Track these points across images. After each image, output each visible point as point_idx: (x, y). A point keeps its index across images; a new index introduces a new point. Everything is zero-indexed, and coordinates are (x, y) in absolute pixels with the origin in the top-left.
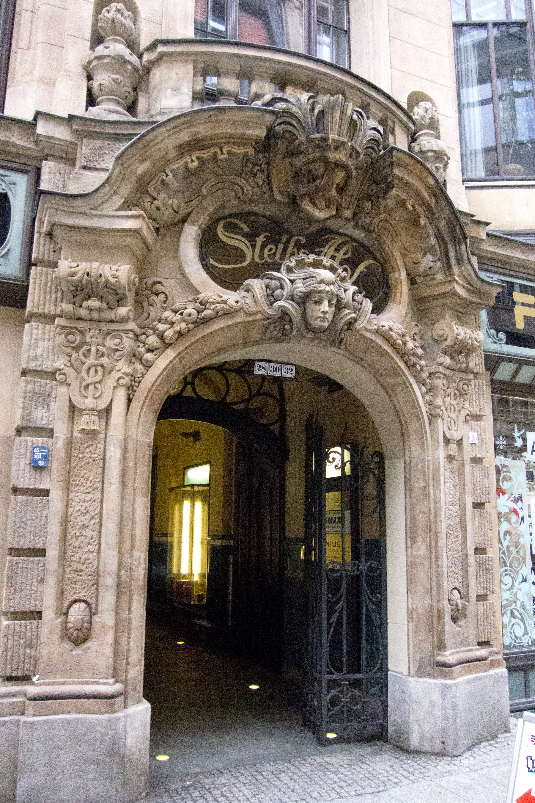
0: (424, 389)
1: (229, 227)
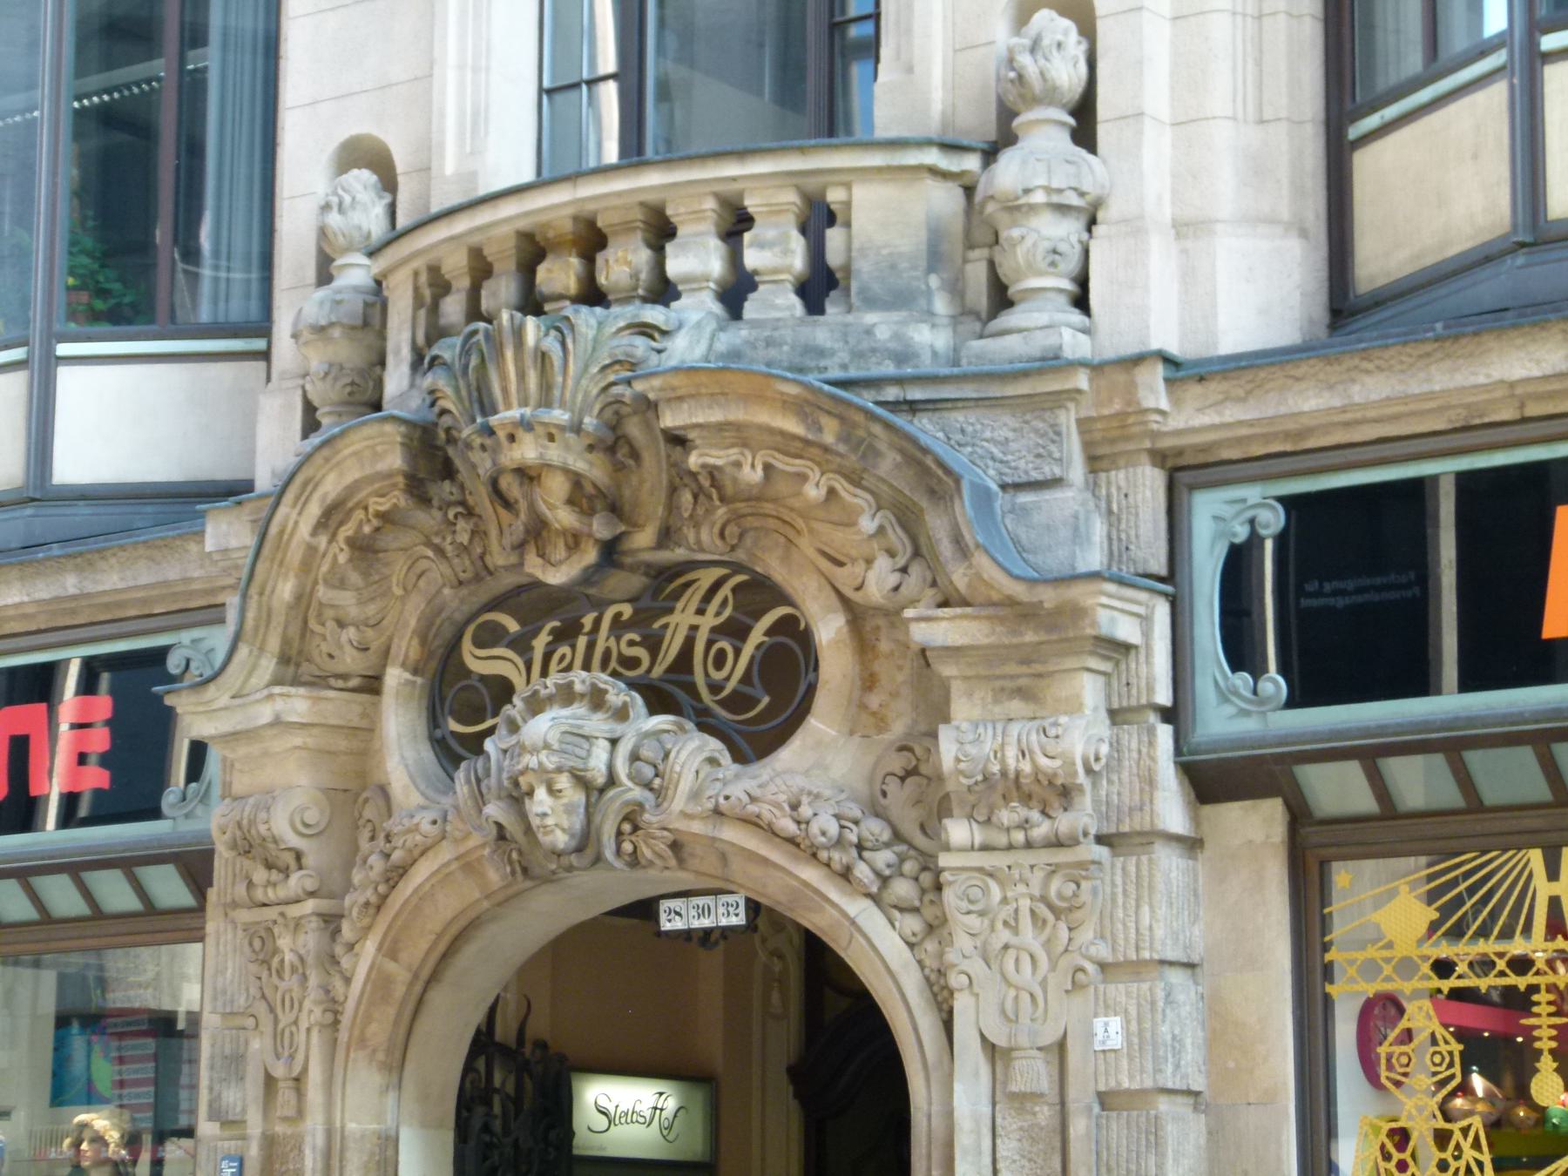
0: (912, 924)
1: (489, 637)
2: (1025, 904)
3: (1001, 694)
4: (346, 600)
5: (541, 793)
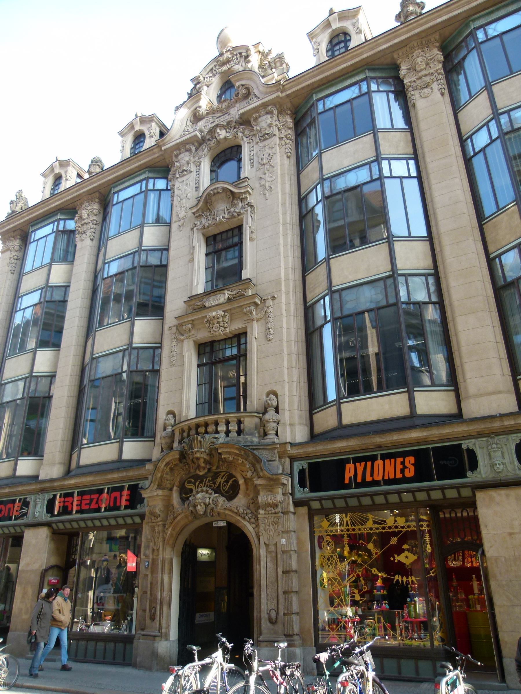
0: (254, 525)
1: (189, 482)
2: (271, 522)
3: (267, 491)
4: (168, 477)
5: (199, 506)
